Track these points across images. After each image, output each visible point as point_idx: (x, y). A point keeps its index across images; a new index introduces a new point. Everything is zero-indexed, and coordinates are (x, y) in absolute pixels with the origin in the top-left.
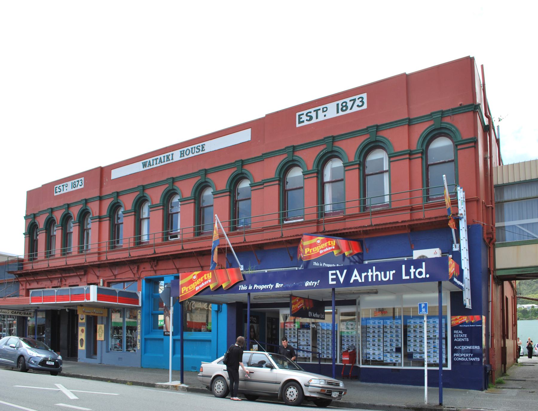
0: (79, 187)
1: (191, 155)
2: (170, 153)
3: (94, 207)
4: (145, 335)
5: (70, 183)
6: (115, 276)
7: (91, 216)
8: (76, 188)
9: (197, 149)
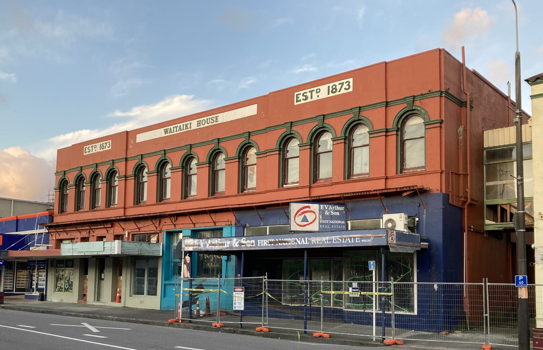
0: (107, 149)
1: (206, 125)
2: (189, 122)
3: (120, 167)
4: (165, 281)
5: (98, 145)
6: (139, 229)
7: (117, 175)
8: (104, 150)
9: (212, 120)
